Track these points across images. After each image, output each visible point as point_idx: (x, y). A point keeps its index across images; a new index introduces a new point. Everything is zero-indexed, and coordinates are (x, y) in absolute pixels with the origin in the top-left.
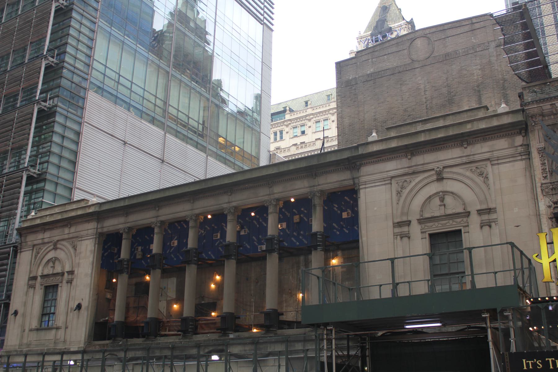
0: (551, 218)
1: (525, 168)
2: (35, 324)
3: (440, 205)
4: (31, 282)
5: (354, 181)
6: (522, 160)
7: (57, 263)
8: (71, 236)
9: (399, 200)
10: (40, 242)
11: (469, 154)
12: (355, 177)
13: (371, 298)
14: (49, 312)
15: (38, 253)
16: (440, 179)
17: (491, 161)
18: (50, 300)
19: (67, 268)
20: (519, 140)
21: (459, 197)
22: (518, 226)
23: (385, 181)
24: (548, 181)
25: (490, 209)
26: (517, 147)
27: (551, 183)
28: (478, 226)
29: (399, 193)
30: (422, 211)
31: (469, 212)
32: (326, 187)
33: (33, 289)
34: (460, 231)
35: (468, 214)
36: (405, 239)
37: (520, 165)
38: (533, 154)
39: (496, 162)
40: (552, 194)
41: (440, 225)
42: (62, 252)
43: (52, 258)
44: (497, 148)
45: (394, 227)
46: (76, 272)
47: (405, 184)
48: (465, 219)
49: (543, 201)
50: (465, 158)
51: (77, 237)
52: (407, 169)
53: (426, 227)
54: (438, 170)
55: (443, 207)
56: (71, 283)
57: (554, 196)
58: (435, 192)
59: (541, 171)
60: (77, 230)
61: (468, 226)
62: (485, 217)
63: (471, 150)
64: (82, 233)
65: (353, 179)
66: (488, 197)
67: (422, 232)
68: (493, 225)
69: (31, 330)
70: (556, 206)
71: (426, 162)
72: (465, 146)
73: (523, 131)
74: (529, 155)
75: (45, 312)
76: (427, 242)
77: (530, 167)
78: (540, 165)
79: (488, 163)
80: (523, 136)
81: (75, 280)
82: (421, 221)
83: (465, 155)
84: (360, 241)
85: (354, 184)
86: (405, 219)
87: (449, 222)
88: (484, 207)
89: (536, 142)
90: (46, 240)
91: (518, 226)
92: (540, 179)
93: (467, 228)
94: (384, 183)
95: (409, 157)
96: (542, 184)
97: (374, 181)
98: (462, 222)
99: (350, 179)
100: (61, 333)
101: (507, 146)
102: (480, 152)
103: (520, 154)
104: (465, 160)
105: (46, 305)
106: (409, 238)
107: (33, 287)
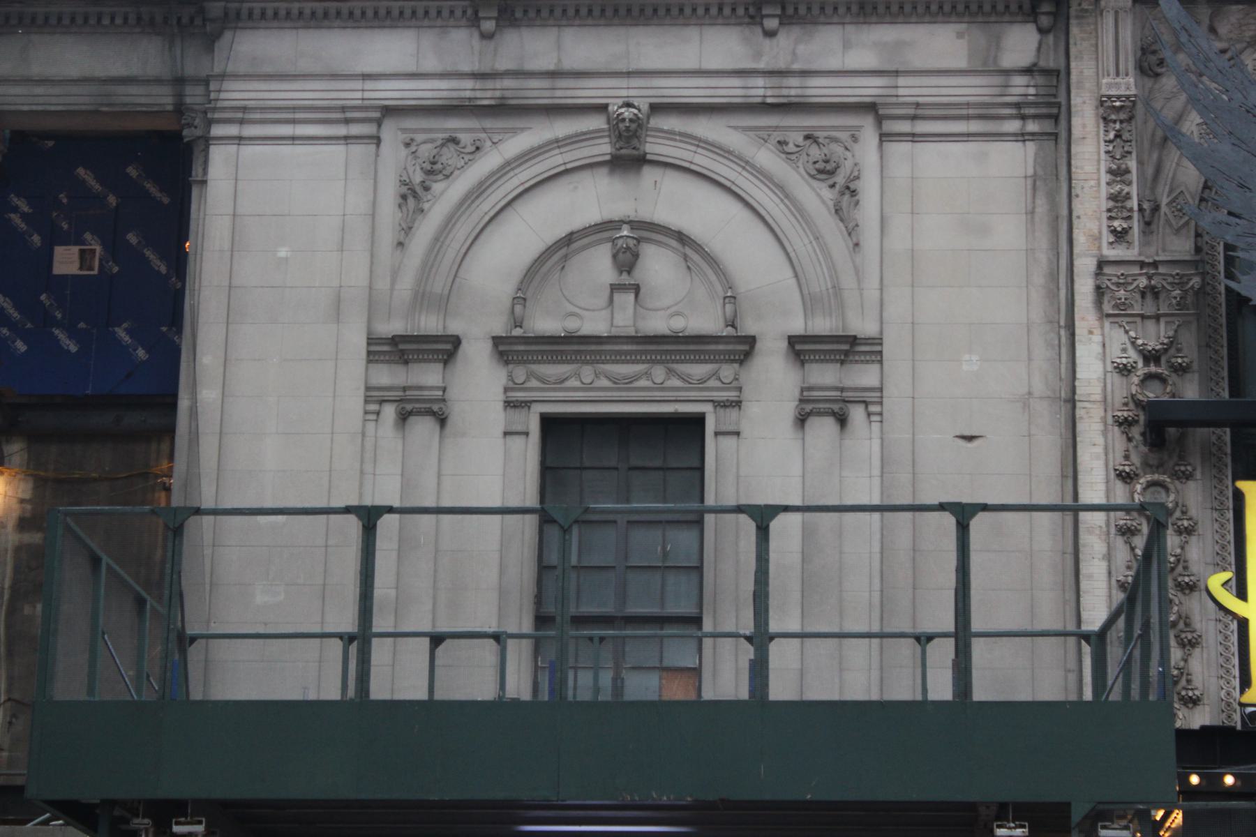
0: (1125, 424)
1: (1035, 177)
3: (615, 288)
5: (180, 96)
6: (1022, 137)
9: (408, 230)
11: (781, 65)
12: (190, 70)
13: (213, 698)
16: (628, 158)
17: (880, 120)
20: (1021, 44)
21: (712, 261)
22: (970, 438)
23: (347, 121)
24: (1131, 253)
25: (853, 340)
26: (1007, 73)
27: (1142, 264)
29: (412, 196)
30: (520, 299)
31: (751, 341)
32: (21, 99)
34: (698, 422)
35: (742, 348)
36: (423, 428)
37: (1011, 161)
38: (1076, 121)
39: (904, 127)
40: (1143, 317)
44: (918, 64)
45: (372, 357)
47: (449, 156)
48: (727, 371)
49: (1097, 338)
50: (760, 82)
52: (469, 84)
53: (534, 383)
54: (627, 113)
55: (632, 296)
57: (1150, 325)
58: (593, 215)
59: (1105, 204)
61: (737, 404)
62: (825, 375)
63: (787, 48)
65: (179, 81)
66: (848, 281)
67: (510, 404)
68: (857, 414)
70: (1153, 369)
71: (568, 65)
72: (772, 23)
73: (1046, 8)
74: (1056, 118)
76: (528, 452)
77: (1054, 178)
78: (1105, 178)
79: (867, 124)
80: (1041, 31)
83: (761, 65)
84: (183, 403)
85: (180, 109)
86: (430, 324)
87: (647, 374)
88: (822, 325)
89: (1100, 70)
91: (970, 438)
92: (1098, 238)
93: (733, 413)
94: (341, 130)
95: (488, 26)
96: (1102, 264)
97: (291, 113)
98: (712, 383)
99: (158, 81)
101: (963, 64)
102: (834, 63)
103: (1020, 110)
104: (759, 89)
106: (442, 421)
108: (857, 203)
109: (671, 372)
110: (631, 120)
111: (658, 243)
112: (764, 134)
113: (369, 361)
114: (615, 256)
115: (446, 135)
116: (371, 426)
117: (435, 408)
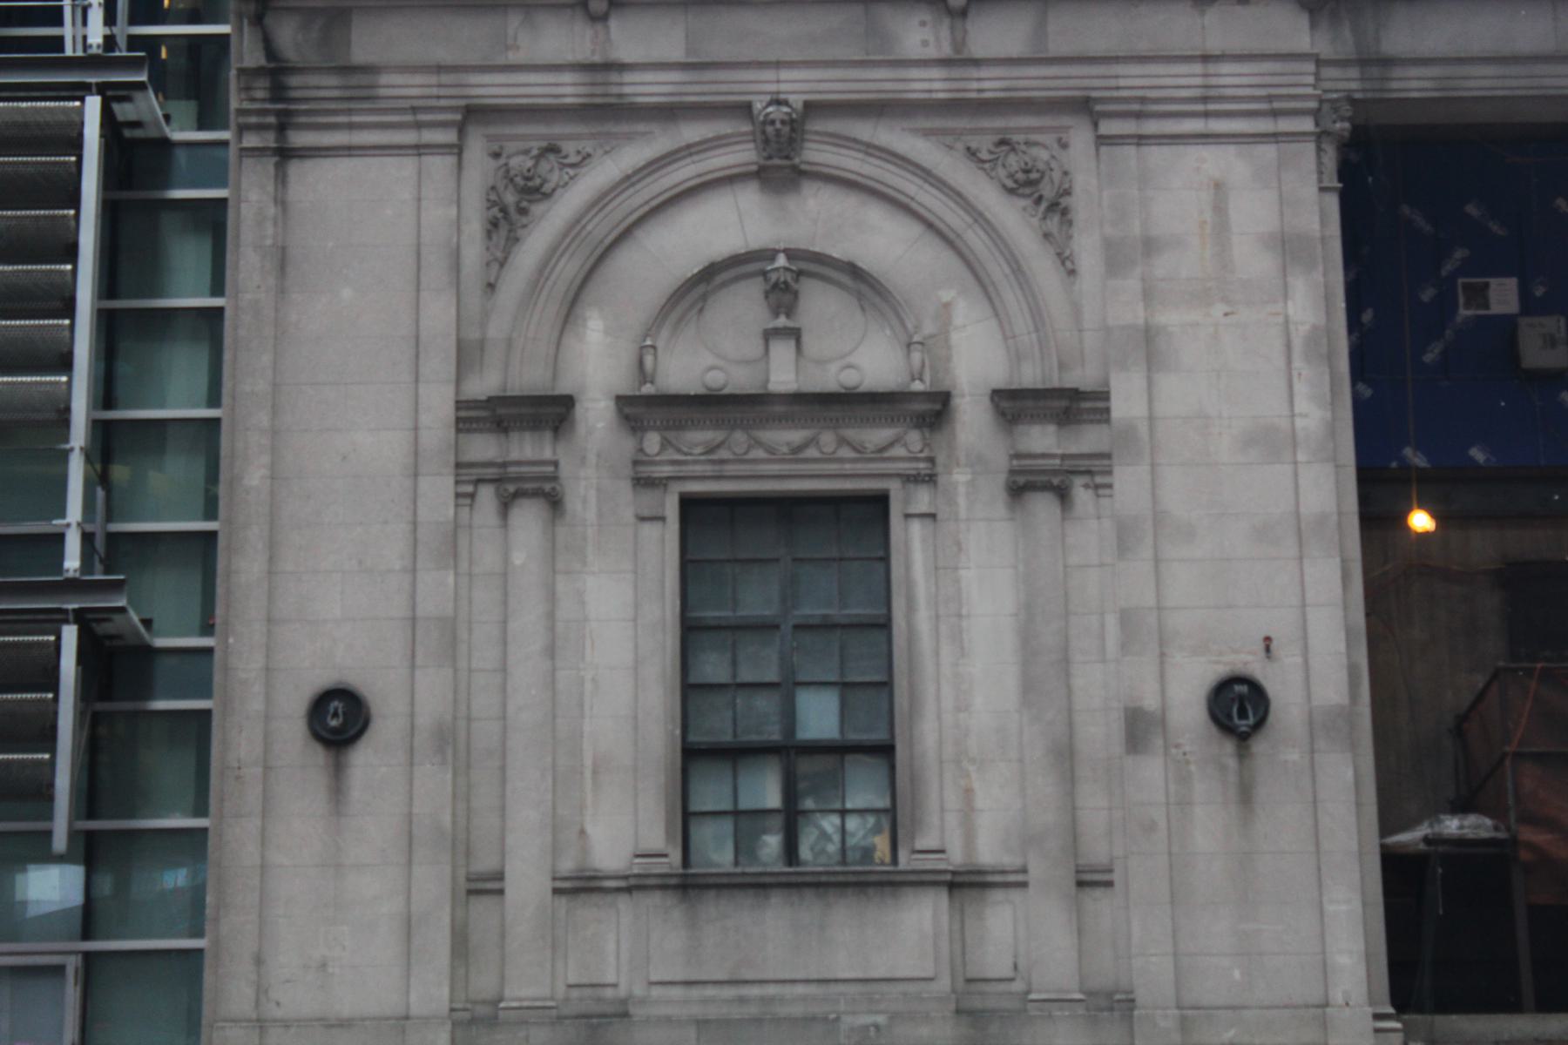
2: (624, 824)
4: (483, 447)
7: (821, 305)
8: (989, 83)
10: (568, 89)
14: (774, 734)
15: (534, 192)
18: (765, 628)
19: (976, 360)
28: (995, 487)
33: (528, 518)
42: (875, 214)
43: (771, 254)
46: (1126, 404)
51: (1084, 106)
56: (1063, 495)
60: (1057, 47)
64: (1133, 78)
69: (582, 886)
75: (717, 727)
81: (1128, 481)
82: (643, 409)
90: (646, 87)
105: (713, 668)
108: (1070, 223)
110: (783, 122)
112: (949, 140)
113: (458, 431)
114: (767, 295)
115: (544, 144)
116: (465, 512)
117: (547, 487)
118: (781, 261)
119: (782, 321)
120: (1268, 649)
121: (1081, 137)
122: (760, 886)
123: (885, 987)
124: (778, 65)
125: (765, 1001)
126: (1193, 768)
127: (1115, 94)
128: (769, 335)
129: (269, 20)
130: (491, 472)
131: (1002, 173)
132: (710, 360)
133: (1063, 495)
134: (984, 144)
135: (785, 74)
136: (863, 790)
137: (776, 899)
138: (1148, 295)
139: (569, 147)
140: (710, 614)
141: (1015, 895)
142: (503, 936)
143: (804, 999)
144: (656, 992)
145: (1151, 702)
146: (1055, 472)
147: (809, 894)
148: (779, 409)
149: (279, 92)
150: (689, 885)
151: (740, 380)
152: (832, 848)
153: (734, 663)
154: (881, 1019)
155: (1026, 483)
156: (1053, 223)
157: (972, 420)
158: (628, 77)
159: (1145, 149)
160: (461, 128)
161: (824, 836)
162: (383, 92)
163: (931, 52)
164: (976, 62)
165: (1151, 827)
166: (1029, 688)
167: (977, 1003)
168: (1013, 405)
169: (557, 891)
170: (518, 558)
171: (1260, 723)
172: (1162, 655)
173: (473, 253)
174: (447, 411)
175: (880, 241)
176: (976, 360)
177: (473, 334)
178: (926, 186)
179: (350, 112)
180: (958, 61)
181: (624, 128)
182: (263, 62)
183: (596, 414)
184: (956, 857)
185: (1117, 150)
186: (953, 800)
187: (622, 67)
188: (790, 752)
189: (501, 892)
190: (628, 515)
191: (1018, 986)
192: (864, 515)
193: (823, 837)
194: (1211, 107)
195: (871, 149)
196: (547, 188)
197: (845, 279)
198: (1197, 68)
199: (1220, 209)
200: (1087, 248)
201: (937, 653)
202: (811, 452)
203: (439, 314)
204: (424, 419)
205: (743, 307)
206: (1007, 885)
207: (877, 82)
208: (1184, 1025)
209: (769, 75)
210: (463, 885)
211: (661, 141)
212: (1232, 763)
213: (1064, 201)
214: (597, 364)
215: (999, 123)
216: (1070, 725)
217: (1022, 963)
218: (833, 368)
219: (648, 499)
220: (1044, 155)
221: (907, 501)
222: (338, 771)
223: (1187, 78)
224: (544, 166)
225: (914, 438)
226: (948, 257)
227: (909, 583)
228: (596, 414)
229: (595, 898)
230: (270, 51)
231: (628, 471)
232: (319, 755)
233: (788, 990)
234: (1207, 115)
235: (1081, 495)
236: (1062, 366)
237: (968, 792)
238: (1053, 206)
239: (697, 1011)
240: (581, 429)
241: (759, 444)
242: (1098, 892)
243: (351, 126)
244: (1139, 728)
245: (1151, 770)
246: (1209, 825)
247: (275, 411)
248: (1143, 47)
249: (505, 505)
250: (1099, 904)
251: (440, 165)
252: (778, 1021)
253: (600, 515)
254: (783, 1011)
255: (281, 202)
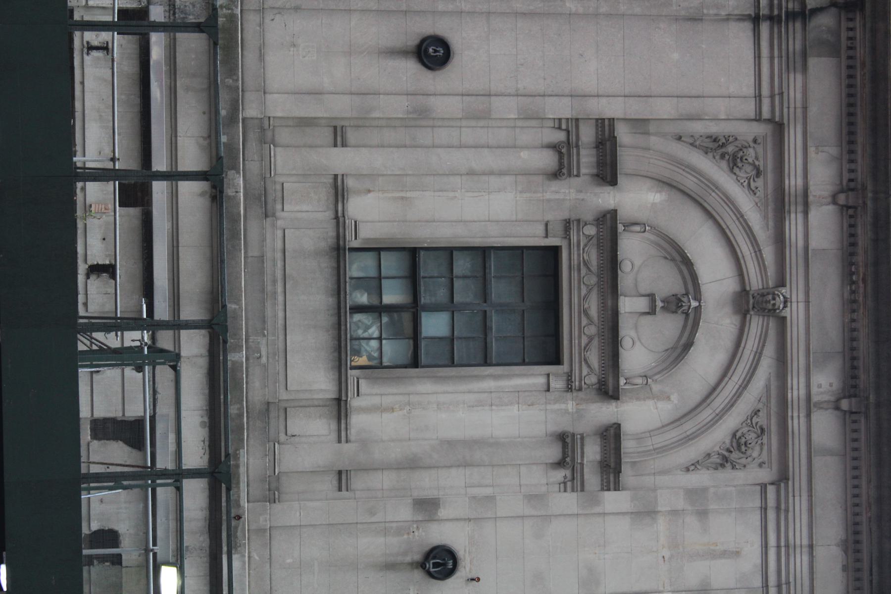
2: (374, 215)
4: (587, 134)
7: (669, 326)
8: (797, 423)
10: (793, 182)
14: (424, 299)
15: (734, 162)
18: (485, 295)
19: (637, 415)
28: (565, 425)
33: (548, 160)
41: (584, 291)
42: (721, 358)
43: (698, 298)
46: (613, 500)
51: (783, 477)
56: (560, 464)
60: (817, 462)
64: (799, 505)
69: (339, 191)
75: (429, 267)
81: (569, 501)
82: (609, 225)
100: (315, 428)
105: (462, 265)
107: (562, 170)
108: (716, 469)
109: (591, 339)
110: (774, 305)
111: (684, 327)
112: (764, 399)
113: (597, 120)
115: (762, 168)
117: (565, 171)
118: (694, 304)
119: (659, 304)
120: (473, 580)
121: (766, 475)
122: (339, 291)
123: (282, 362)
124: (807, 302)
125: (275, 293)
126: (406, 536)
127: (791, 495)
128: (652, 297)
129: (833, 10)
130: (573, 138)
131: (745, 430)
132: (637, 263)
133: (560, 464)
134: (761, 420)
135: (802, 306)
136: (393, 350)
137: (332, 301)
138: (675, 513)
139: (760, 182)
140: (492, 263)
141: (334, 436)
142: (311, 147)
143: (275, 316)
144: (279, 233)
145: (442, 513)
146: (573, 459)
147: (334, 319)
148: (609, 303)
149: (792, 16)
150: (339, 251)
151: (626, 281)
152: (360, 332)
153: (465, 277)
154: (264, 360)
155: (567, 443)
156: (715, 459)
157: (603, 413)
158: (800, 216)
159: (759, 512)
160: (770, 121)
161: (367, 328)
162: (792, 76)
163: (814, 390)
164: (809, 415)
165: (372, 512)
166: (450, 444)
167: (273, 414)
168: (612, 436)
169: (336, 176)
170: (524, 154)
171: (431, 575)
172: (469, 520)
173: (699, 128)
174: (608, 114)
175: (706, 360)
176: (637, 415)
177: (652, 128)
178: (737, 386)
179: (780, 57)
180: (809, 406)
181: (771, 215)
182: (809, 7)
183: (606, 198)
184: (355, 403)
185: (758, 497)
186: (387, 401)
187: (806, 213)
188: (414, 309)
189: (335, 145)
190: (549, 217)
191: (282, 437)
192: (549, 352)
193: (367, 327)
194: (783, 549)
195: (758, 355)
196: (736, 170)
197: (684, 340)
198: (805, 542)
199: (724, 554)
200: (702, 478)
201: (469, 392)
202: (584, 321)
203: (664, 109)
204: (604, 100)
205: (668, 282)
206: (339, 431)
207: (797, 358)
208: (261, 531)
209: (801, 297)
210: (339, 124)
211: (763, 234)
212: (408, 559)
213: (728, 465)
214: (635, 198)
215: (774, 428)
216: (430, 467)
217: (297, 439)
218: (633, 333)
219: (558, 228)
220: (755, 454)
221: (557, 375)
222: (403, 53)
223: (800, 536)
224: (749, 168)
225: (593, 379)
226: (698, 398)
227: (509, 376)
228: (606, 198)
229: (332, 199)
230: (815, 11)
231: (573, 217)
232: (413, 42)
233: (280, 307)
234: (778, 547)
235: (560, 475)
236: (634, 463)
237: (392, 410)
238: (726, 459)
239: (269, 255)
240: (598, 190)
241: (589, 291)
242: (335, 483)
243: (772, 58)
244: (427, 507)
245: (404, 513)
246: (373, 545)
247: (608, 15)
248: (818, 511)
249: (554, 147)
250: (328, 484)
251: (750, 109)
252: (263, 302)
253: (549, 201)
254: (268, 304)
255: (728, 18)
